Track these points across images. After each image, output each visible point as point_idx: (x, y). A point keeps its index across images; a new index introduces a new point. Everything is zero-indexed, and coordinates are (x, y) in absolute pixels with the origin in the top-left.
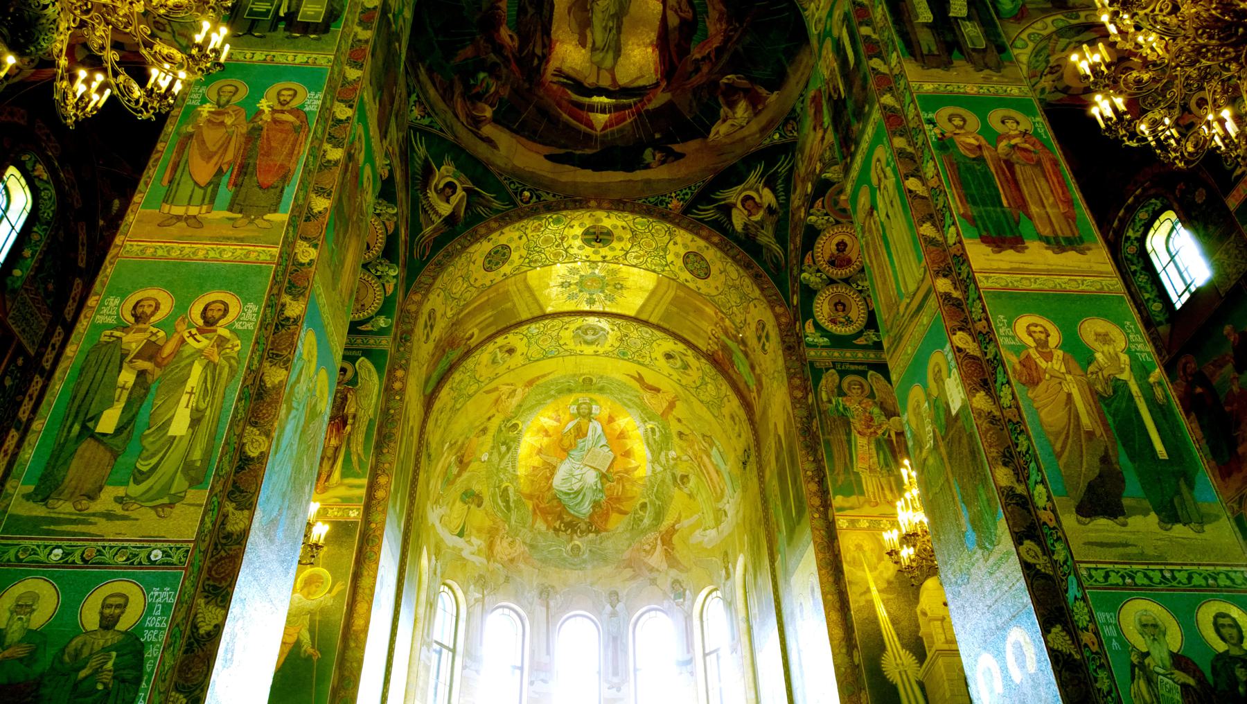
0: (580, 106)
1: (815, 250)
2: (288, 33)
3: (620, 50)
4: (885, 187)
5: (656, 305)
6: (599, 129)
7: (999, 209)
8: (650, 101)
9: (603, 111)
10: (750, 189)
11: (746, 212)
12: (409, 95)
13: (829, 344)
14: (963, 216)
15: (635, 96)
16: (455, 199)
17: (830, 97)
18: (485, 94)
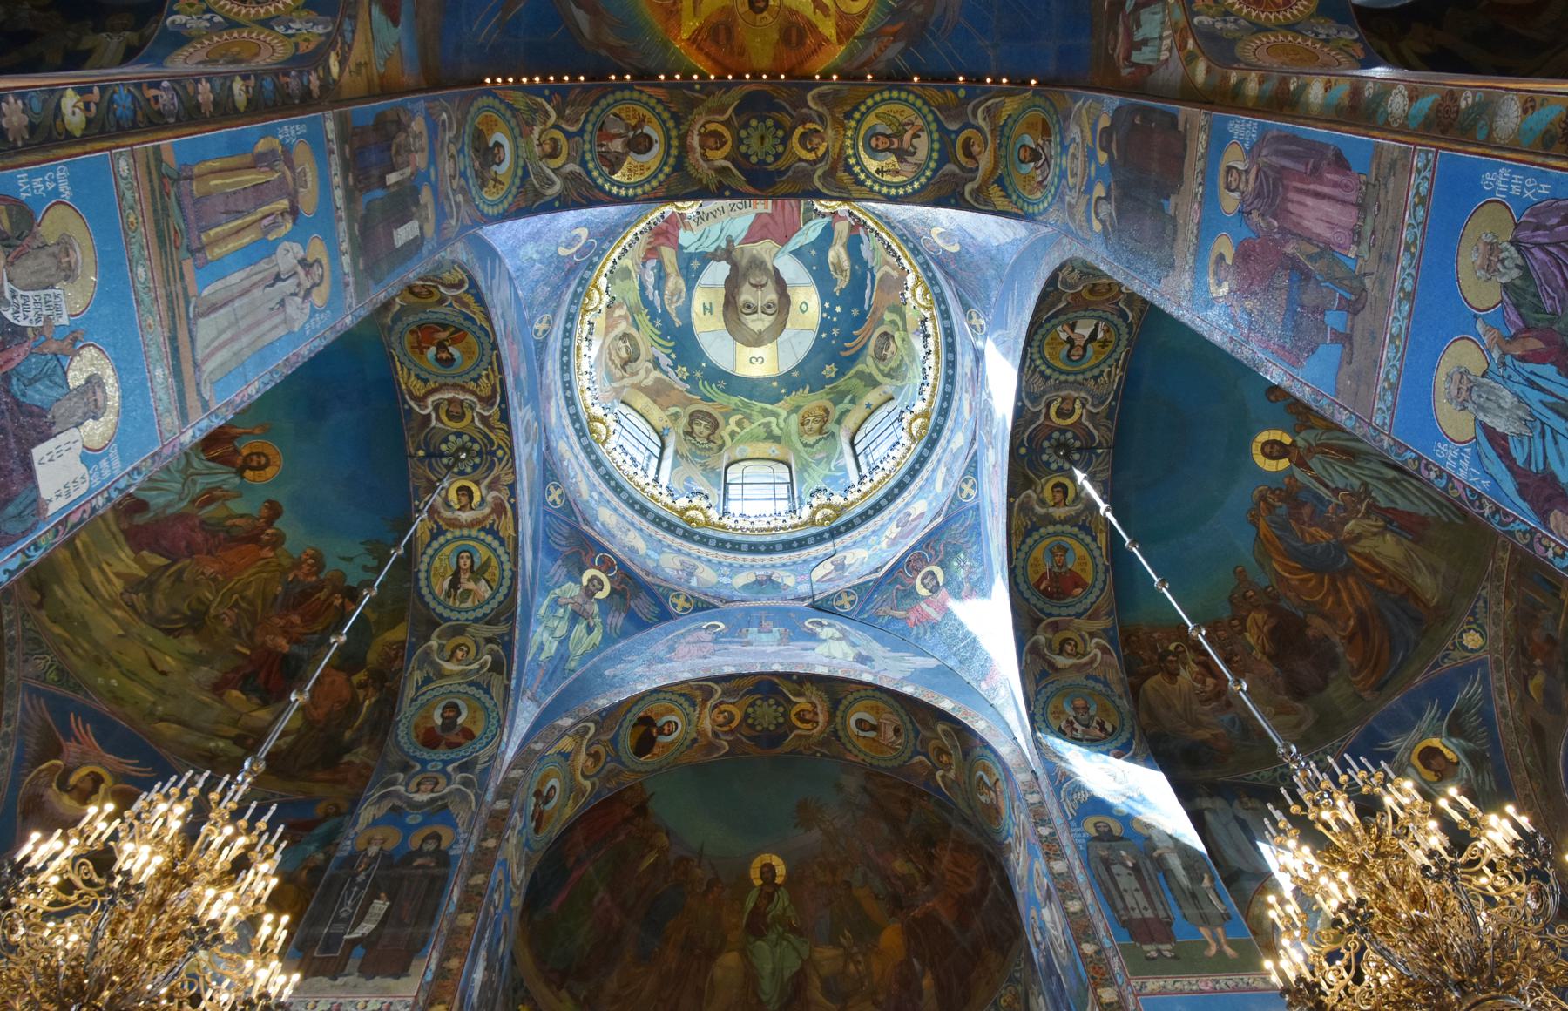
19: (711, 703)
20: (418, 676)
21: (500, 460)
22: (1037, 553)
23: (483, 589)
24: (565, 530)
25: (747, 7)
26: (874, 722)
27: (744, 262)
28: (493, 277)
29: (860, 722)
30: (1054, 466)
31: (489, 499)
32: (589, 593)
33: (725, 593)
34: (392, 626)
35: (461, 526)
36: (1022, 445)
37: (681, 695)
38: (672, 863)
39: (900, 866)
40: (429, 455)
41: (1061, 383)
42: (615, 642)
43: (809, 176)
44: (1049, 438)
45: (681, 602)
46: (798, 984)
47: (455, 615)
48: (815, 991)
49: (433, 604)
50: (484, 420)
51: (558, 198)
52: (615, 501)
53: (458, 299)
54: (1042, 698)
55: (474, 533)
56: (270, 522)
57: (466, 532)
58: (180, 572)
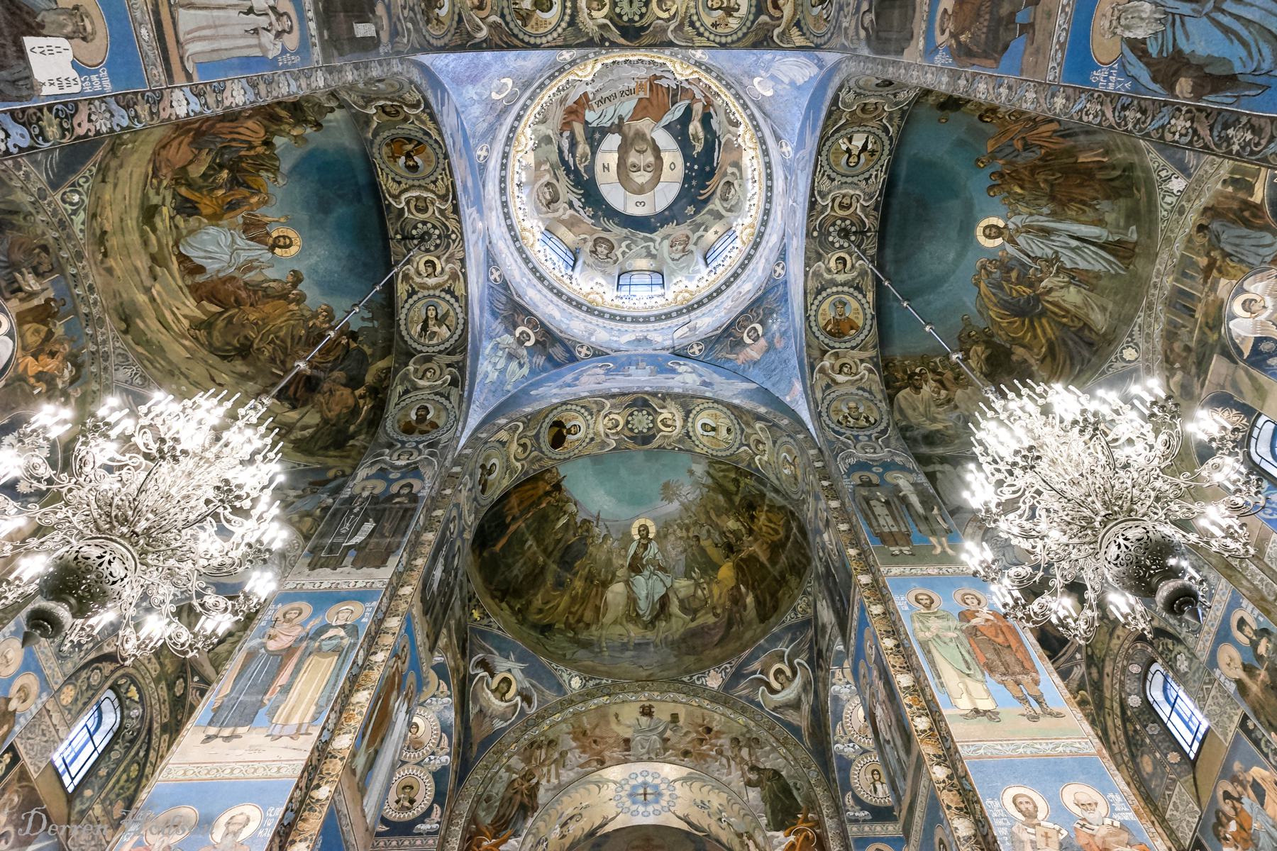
20: (400, 389)
21: (454, 241)
22: (826, 305)
23: (445, 333)
24: (503, 299)
28: (443, 105)
29: (704, 425)
32: (520, 342)
33: (615, 346)
34: (383, 358)
35: (428, 288)
36: (814, 229)
39: (732, 524)
40: (404, 238)
42: (539, 374)
44: (834, 224)
45: (584, 351)
46: (664, 601)
47: (425, 349)
48: (675, 608)
49: (410, 342)
50: (442, 212)
51: (485, 41)
52: (540, 286)
53: (418, 117)
54: (826, 403)
56: (295, 285)
57: (431, 292)
58: (231, 317)
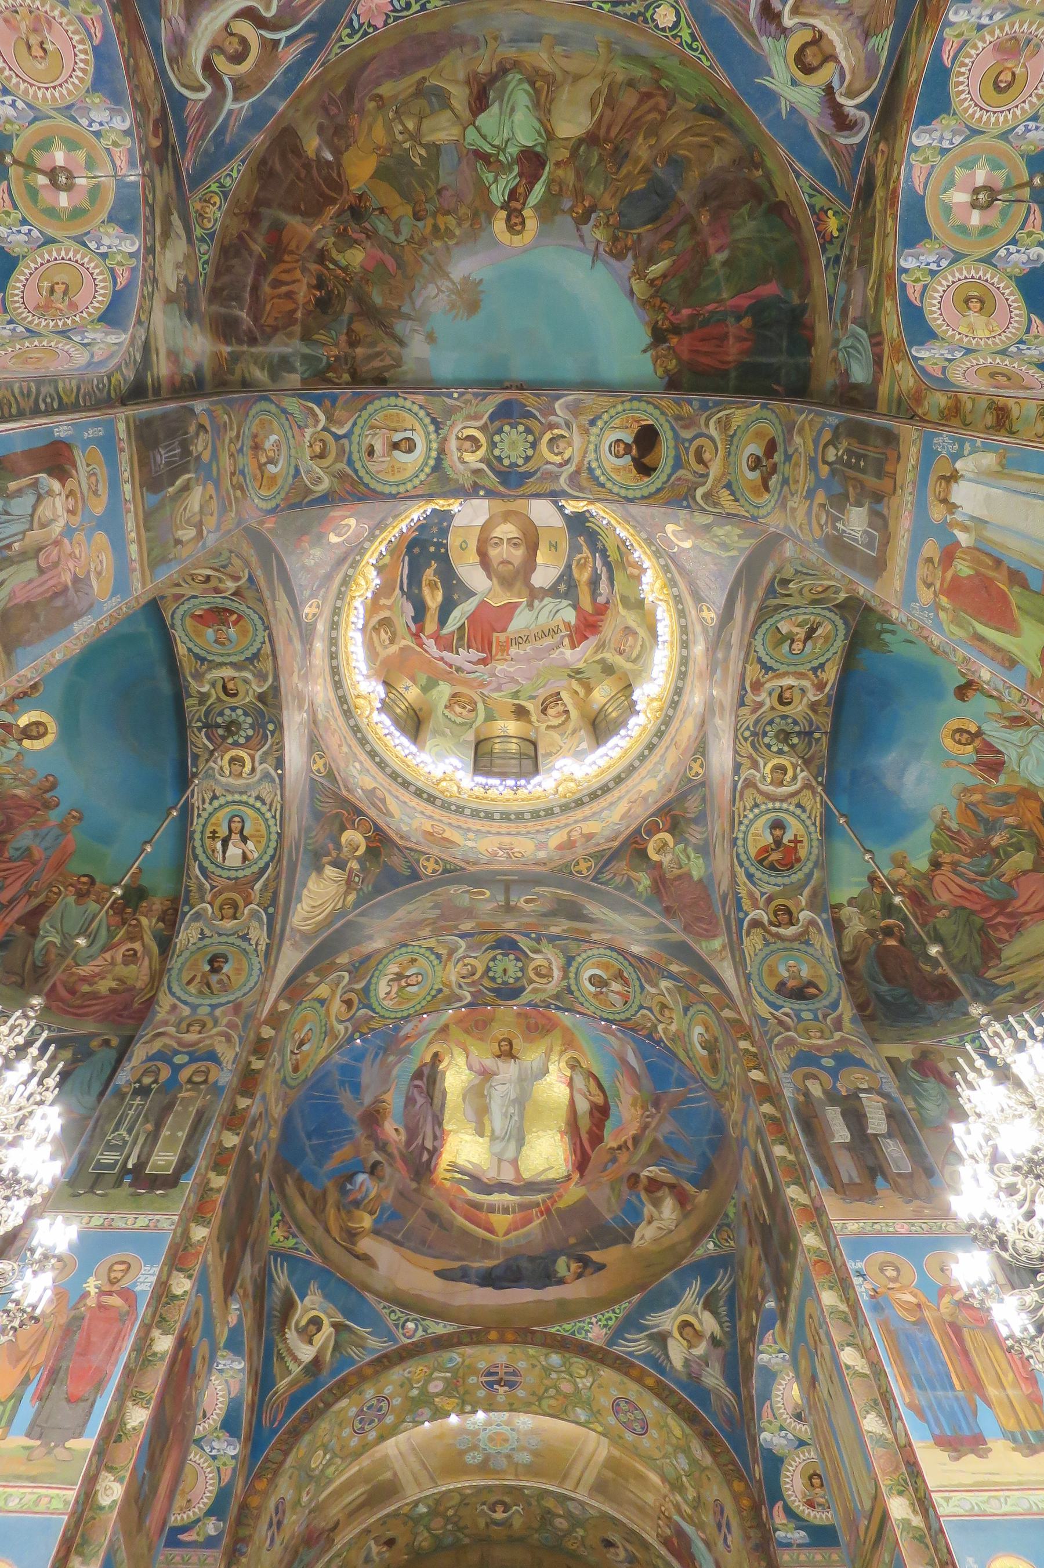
0: (476, 1206)
1: (774, 1399)
2: (132, 1190)
3: (524, 1139)
4: (822, 1355)
5: (585, 1468)
6: (501, 1233)
7: (950, 1394)
8: (560, 1196)
9: (506, 1211)
10: (685, 1312)
11: (685, 1343)
12: (272, 1215)
13: (807, 1540)
14: (911, 1406)
15: (543, 1191)
16: (319, 1339)
17: (756, 1218)
18: (364, 1199)
19: (571, 468)
21: (748, 728)
25: (514, 1042)
26: (396, 453)
27: (518, 585)
29: (410, 450)
30: (240, 712)
31: (763, 696)
37: (603, 486)
38: (630, 255)
40: (810, 734)
41: (245, 793)
43: (469, 947)
50: (755, 765)
55: (783, 668)
